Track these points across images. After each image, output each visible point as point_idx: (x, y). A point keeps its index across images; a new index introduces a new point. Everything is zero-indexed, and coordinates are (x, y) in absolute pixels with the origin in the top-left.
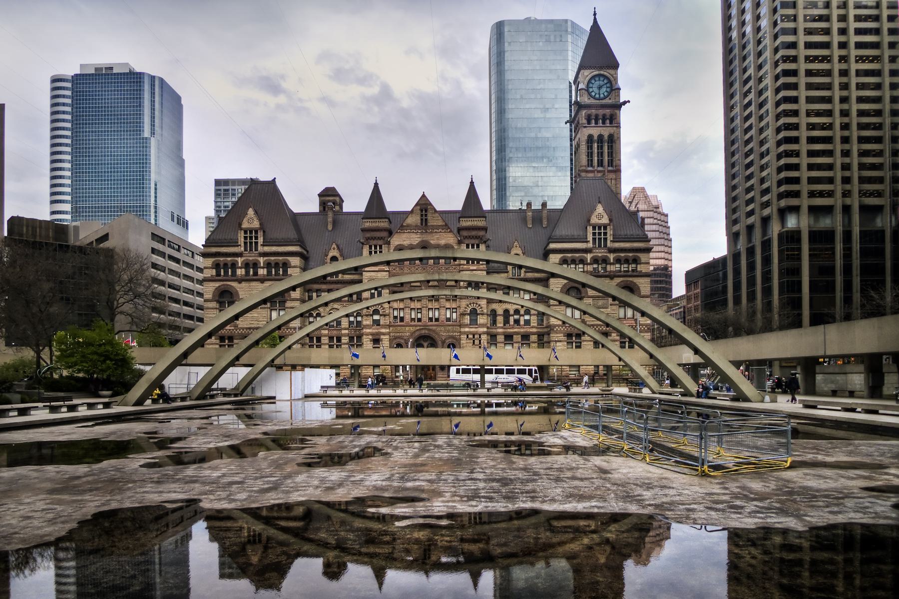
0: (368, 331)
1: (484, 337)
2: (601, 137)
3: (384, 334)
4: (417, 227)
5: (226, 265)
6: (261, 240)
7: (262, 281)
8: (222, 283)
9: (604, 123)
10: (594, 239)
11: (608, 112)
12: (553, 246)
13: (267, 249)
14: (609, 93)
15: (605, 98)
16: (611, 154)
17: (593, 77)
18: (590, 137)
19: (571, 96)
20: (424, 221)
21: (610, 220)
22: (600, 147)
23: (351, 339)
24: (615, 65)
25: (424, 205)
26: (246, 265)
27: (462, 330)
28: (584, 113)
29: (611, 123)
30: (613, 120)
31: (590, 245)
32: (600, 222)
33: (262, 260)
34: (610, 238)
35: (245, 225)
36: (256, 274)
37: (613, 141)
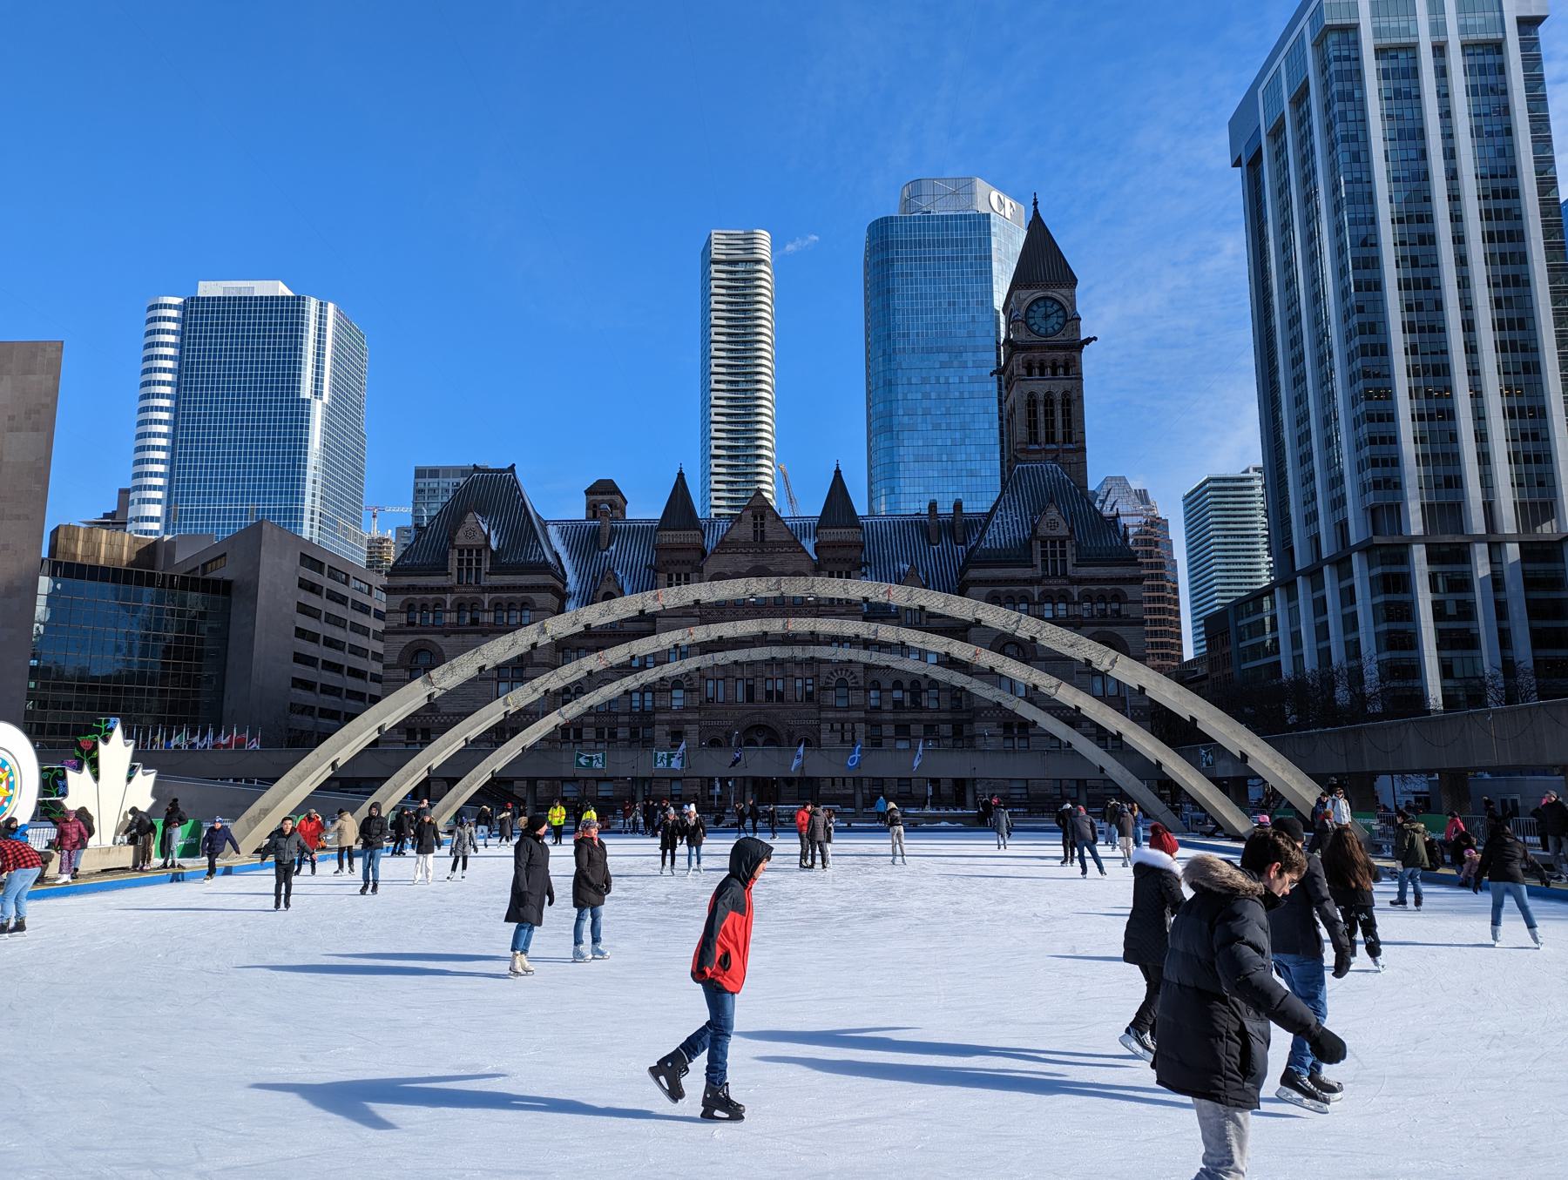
0: (664, 717)
1: (861, 728)
2: (1049, 394)
3: (689, 722)
4: (746, 544)
5: (424, 606)
8: (417, 637)
9: (1054, 373)
10: (1045, 561)
11: (1060, 356)
12: (973, 573)
13: (496, 580)
14: (1063, 326)
15: (1055, 333)
16: (1067, 423)
17: (1035, 301)
18: (1031, 394)
19: (998, 333)
20: (759, 535)
21: (1071, 530)
22: (1050, 413)
24: (1072, 281)
26: (460, 607)
27: (823, 715)
28: (1019, 358)
29: (1066, 373)
30: (1070, 368)
31: (1039, 572)
32: (1054, 533)
33: (487, 598)
34: (1071, 560)
36: (475, 621)
37: (1071, 405)
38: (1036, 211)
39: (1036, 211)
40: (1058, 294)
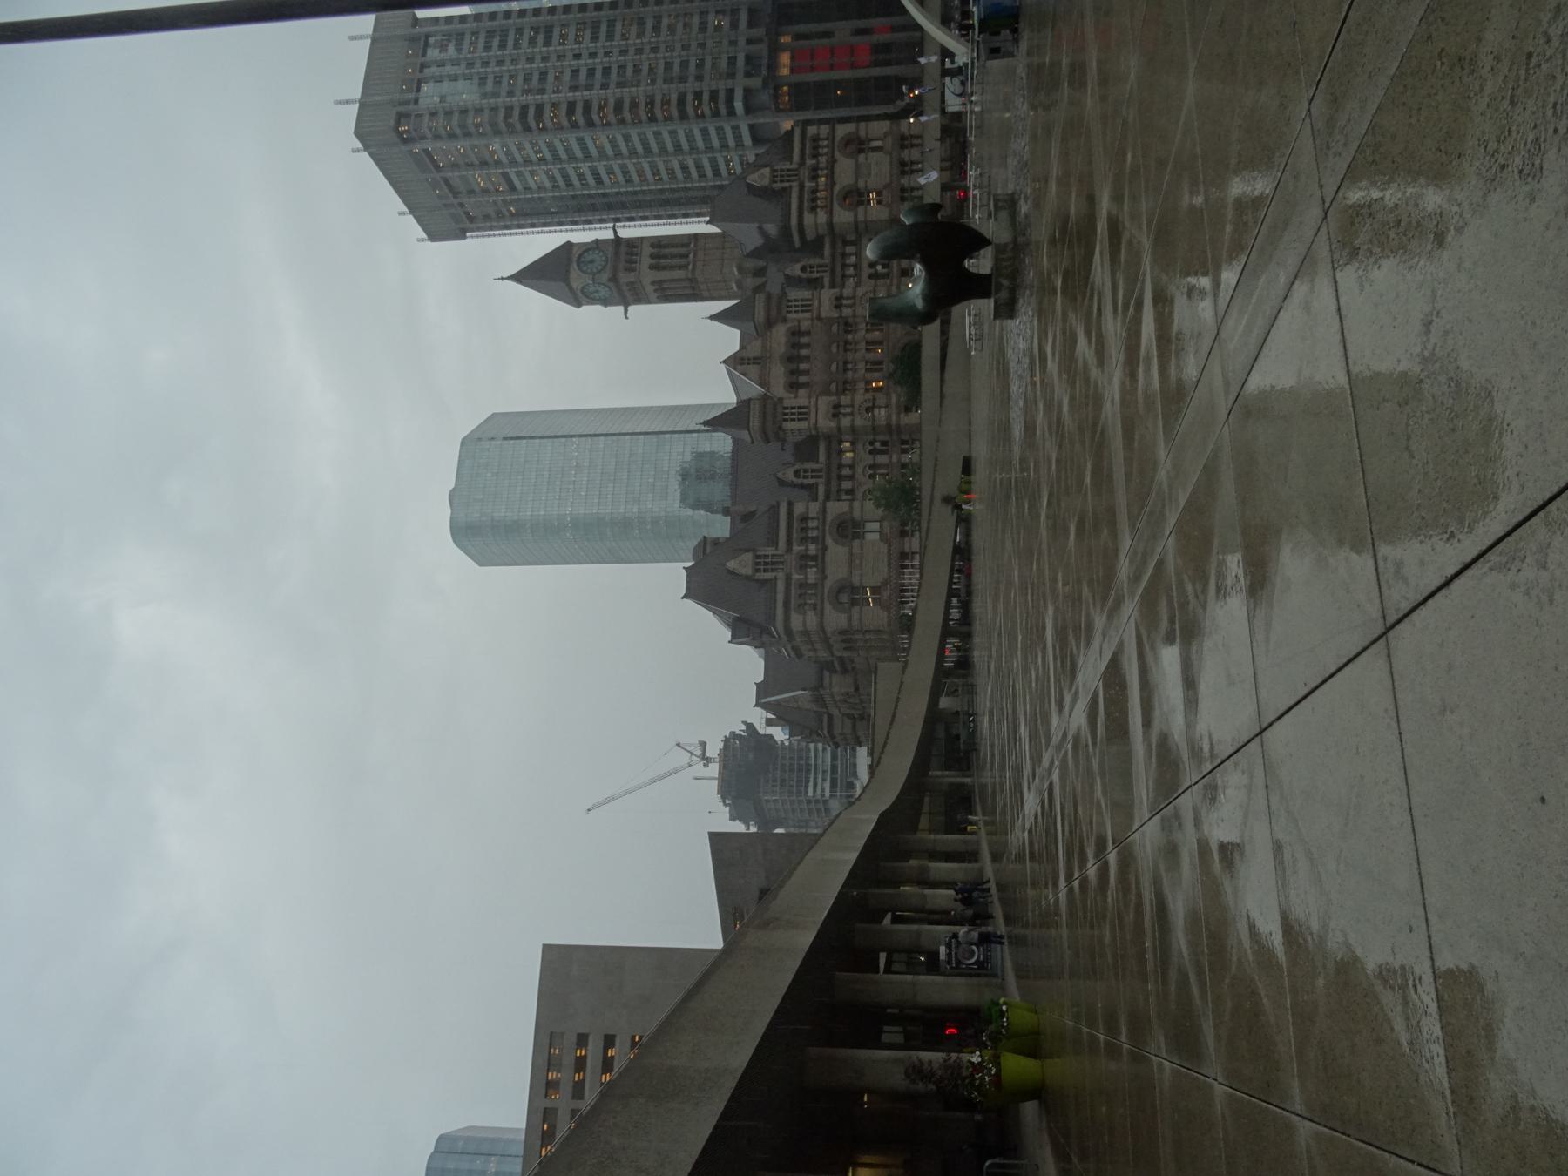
0: (894, 418)
2: (652, 256)
6: (770, 551)
7: (825, 548)
18: (652, 267)
20: (756, 361)
22: (665, 257)
23: (905, 451)
25: (736, 362)
26: (802, 568)
33: (797, 548)
35: (748, 571)
36: (814, 558)
38: (508, 278)
39: (508, 278)
40: (576, 253)
